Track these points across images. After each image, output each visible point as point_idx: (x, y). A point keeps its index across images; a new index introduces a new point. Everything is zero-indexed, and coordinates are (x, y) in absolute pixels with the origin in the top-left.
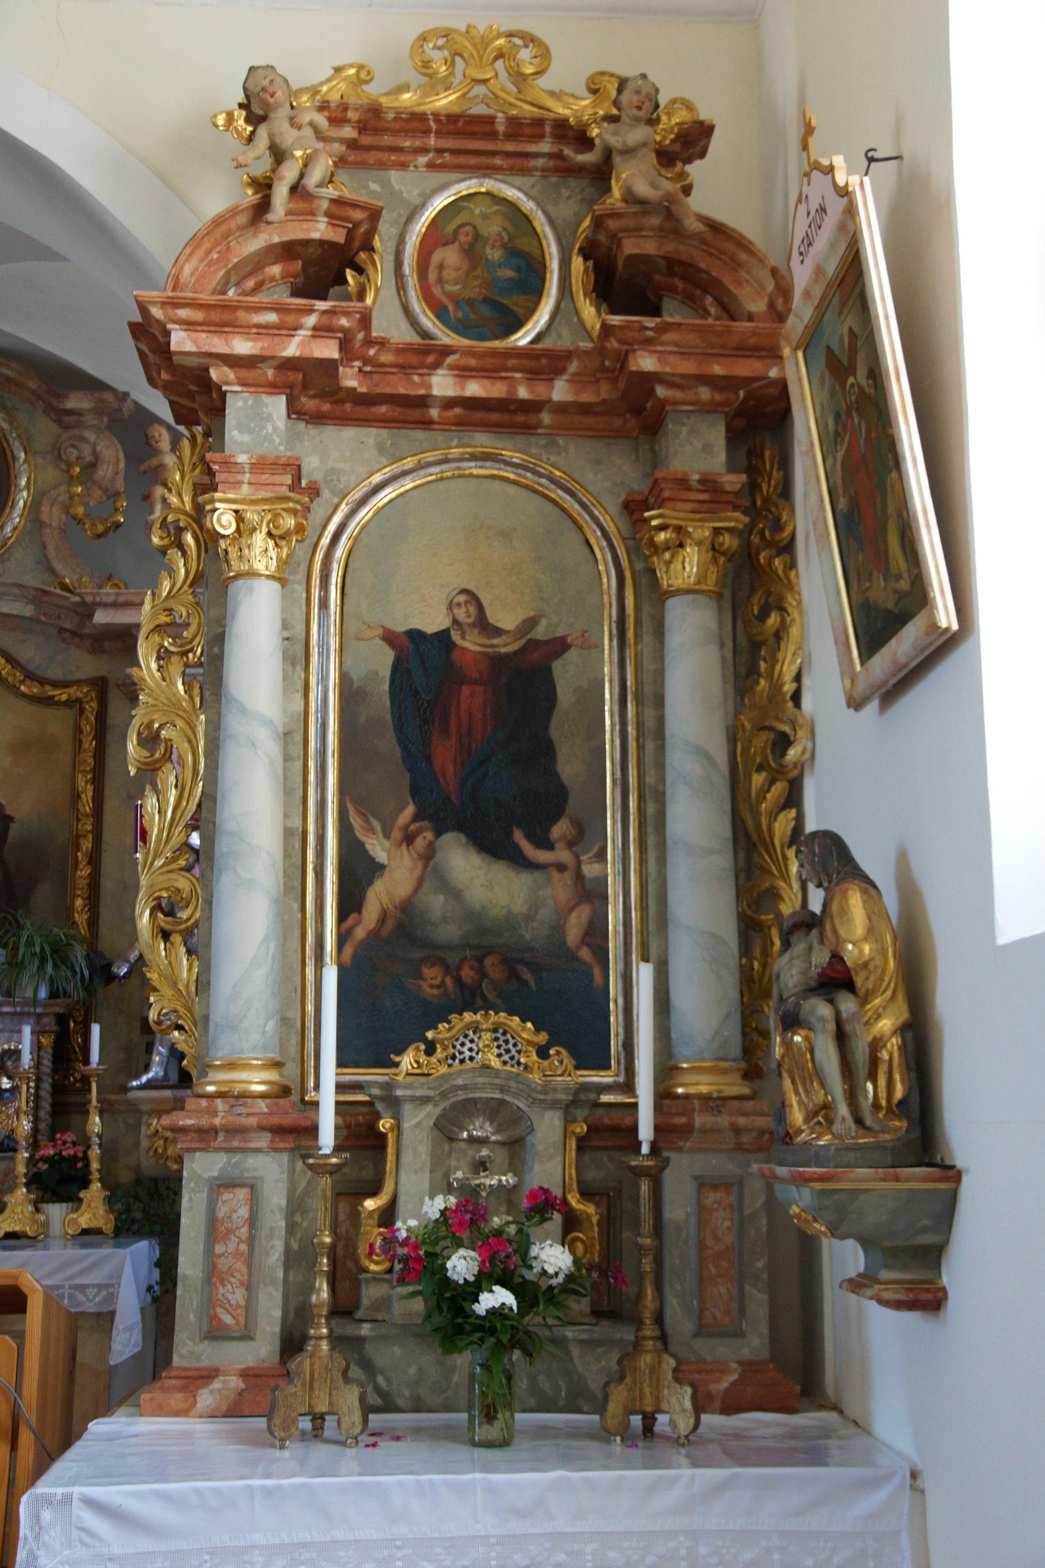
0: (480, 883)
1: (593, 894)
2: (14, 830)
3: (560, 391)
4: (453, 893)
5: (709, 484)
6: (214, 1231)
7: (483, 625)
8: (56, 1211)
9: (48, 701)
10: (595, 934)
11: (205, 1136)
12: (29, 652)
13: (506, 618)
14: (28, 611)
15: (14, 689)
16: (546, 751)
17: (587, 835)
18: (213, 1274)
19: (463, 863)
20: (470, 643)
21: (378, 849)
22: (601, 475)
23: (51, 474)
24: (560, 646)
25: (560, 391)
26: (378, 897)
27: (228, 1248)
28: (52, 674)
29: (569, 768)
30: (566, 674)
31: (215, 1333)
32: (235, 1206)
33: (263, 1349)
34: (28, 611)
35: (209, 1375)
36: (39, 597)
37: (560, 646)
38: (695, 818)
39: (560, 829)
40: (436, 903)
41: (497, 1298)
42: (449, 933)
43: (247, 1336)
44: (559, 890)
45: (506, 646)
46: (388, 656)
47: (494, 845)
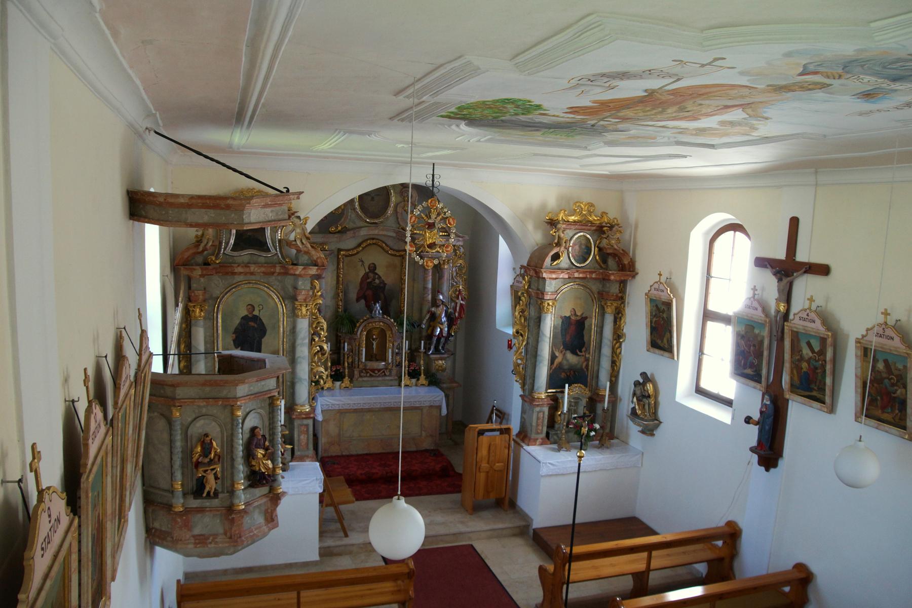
0: (572, 359)
1: (587, 360)
2: (387, 287)
3: (594, 276)
4: (568, 361)
5: (617, 296)
6: (538, 418)
7: (575, 315)
8: (414, 381)
9: (395, 255)
10: (587, 366)
11: (538, 405)
12: (390, 243)
13: (579, 314)
14: (394, 235)
15: (387, 252)
16: (583, 336)
17: (588, 350)
18: (538, 425)
19: (570, 356)
20: (573, 318)
21: (557, 354)
22: (595, 287)
23: (400, 199)
24: (586, 318)
25: (594, 276)
26: (557, 361)
27: (540, 421)
28: (396, 248)
29: (586, 339)
30: (587, 323)
31: (538, 433)
32: (541, 415)
33: (544, 435)
34: (394, 235)
35: (536, 440)
36: (397, 233)
37: (586, 318)
38: (606, 351)
39: (584, 349)
40: (565, 362)
41: (593, 433)
42: (566, 367)
43: (542, 433)
44: (582, 359)
45: (578, 318)
46: (561, 321)
47: (574, 353)
